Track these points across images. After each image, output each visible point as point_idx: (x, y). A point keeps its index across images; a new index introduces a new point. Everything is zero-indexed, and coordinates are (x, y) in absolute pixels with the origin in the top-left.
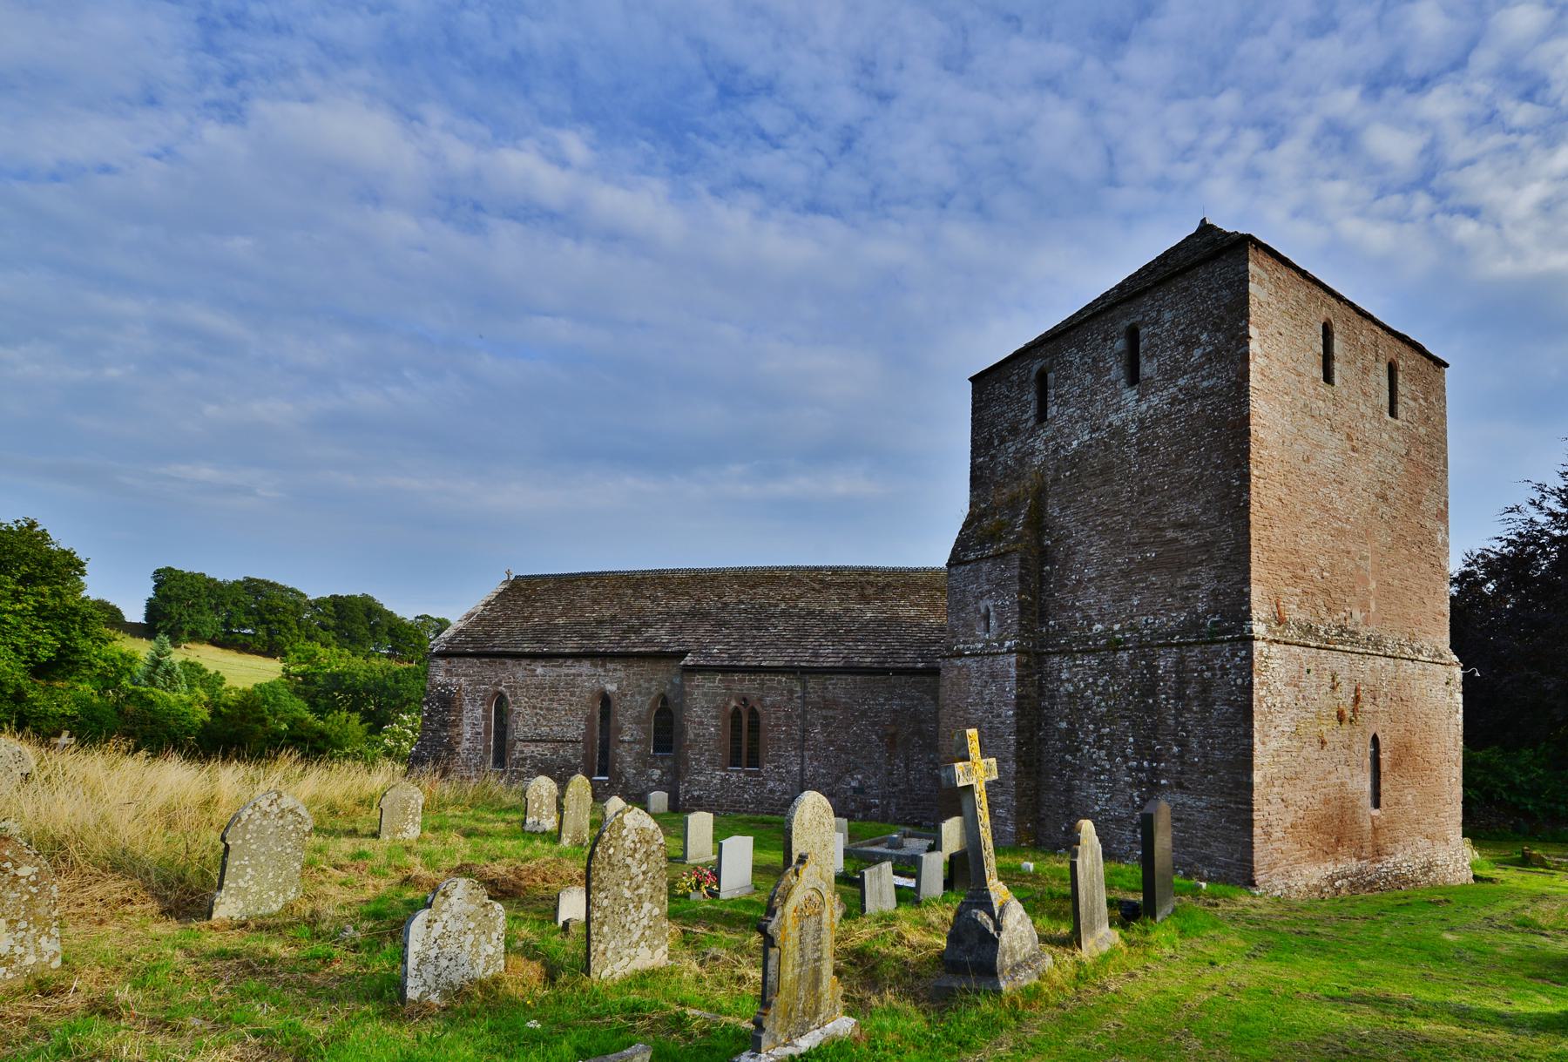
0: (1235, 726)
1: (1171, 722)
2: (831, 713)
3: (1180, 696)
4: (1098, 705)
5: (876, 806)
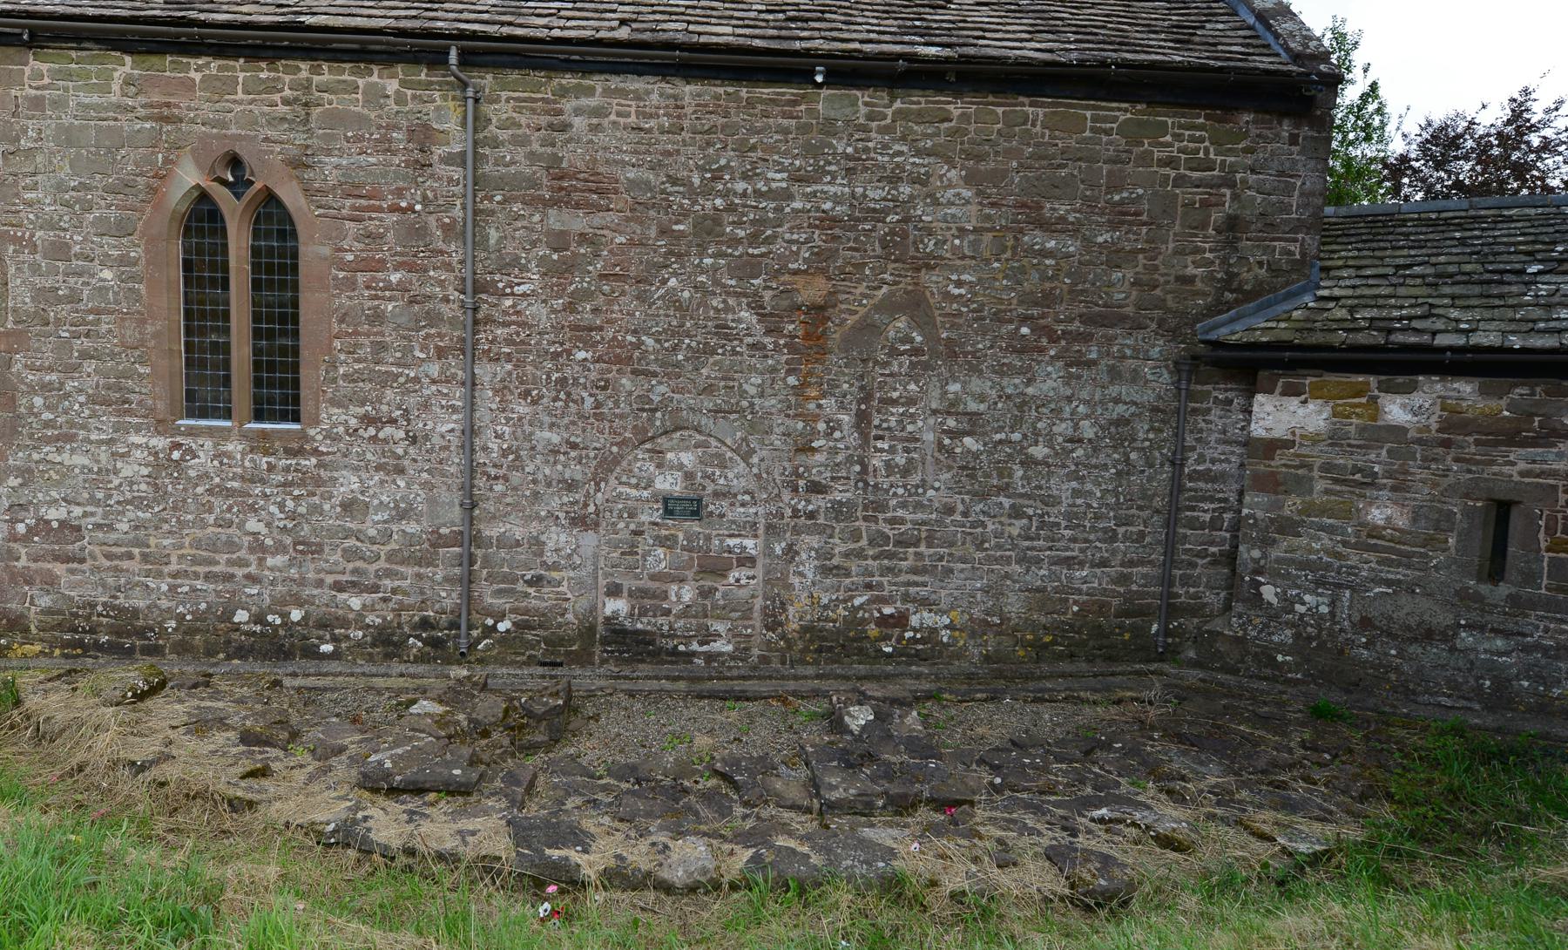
2: (578, 222)
5: (747, 561)
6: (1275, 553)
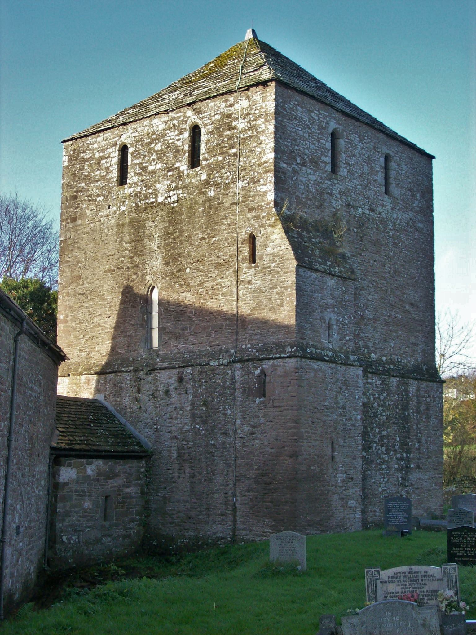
0: (438, 430)
1: (415, 427)
3: (418, 412)
4: (381, 415)
6: (65, 524)
